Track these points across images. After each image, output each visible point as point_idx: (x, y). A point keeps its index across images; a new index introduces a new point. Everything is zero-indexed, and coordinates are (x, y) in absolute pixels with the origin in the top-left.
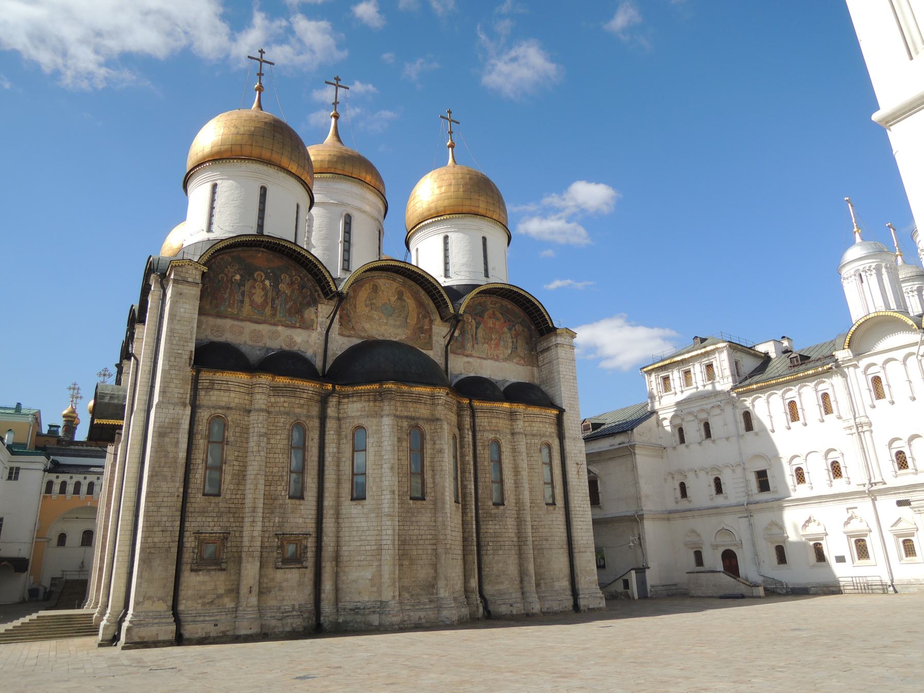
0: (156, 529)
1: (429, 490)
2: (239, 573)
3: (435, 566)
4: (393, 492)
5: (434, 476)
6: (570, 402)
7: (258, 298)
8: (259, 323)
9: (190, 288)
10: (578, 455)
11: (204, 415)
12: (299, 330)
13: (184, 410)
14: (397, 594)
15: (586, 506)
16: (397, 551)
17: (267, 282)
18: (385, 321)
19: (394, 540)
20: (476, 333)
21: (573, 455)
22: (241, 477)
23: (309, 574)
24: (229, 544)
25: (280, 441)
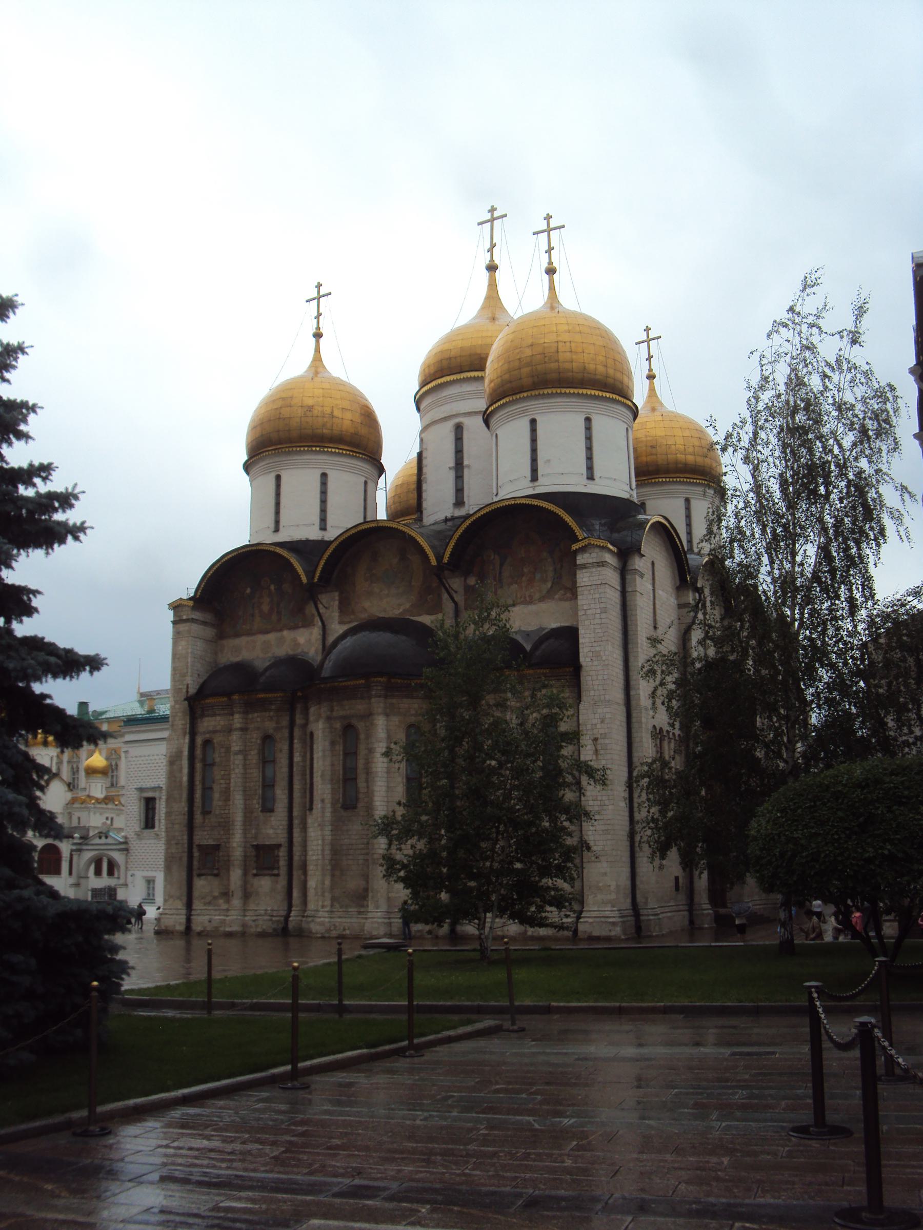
0: (173, 842)
1: (361, 796)
2: (228, 880)
3: (366, 877)
4: (323, 801)
5: (367, 781)
6: (593, 649)
7: (266, 608)
8: (266, 632)
9: (184, 625)
10: (598, 726)
11: (199, 740)
12: (302, 630)
13: (184, 739)
14: (328, 903)
15: (604, 798)
16: (327, 862)
17: (272, 587)
18: (386, 592)
19: (323, 850)
20: (500, 573)
21: (589, 727)
22: (227, 794)
23: (282, 881)
24: (221, 854)
25: (254, 757)
